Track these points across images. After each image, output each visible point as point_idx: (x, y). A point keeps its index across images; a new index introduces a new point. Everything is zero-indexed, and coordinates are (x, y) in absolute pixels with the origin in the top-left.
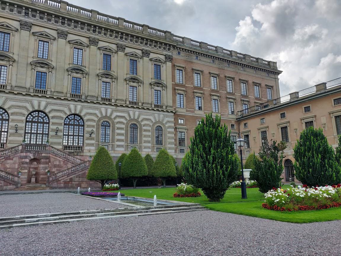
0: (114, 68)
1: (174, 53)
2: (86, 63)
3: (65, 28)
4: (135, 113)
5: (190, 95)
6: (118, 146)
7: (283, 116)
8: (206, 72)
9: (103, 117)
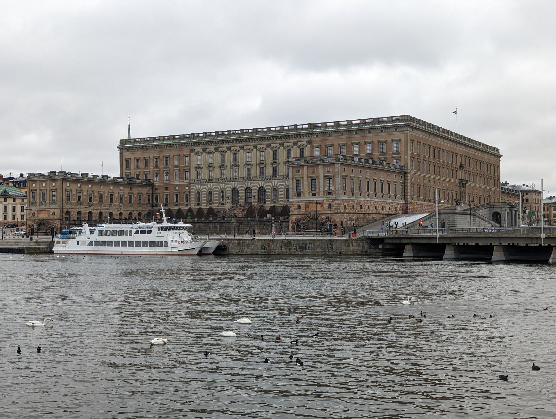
1: (314, 138)
6: (281, 201)
9: (273, 186)
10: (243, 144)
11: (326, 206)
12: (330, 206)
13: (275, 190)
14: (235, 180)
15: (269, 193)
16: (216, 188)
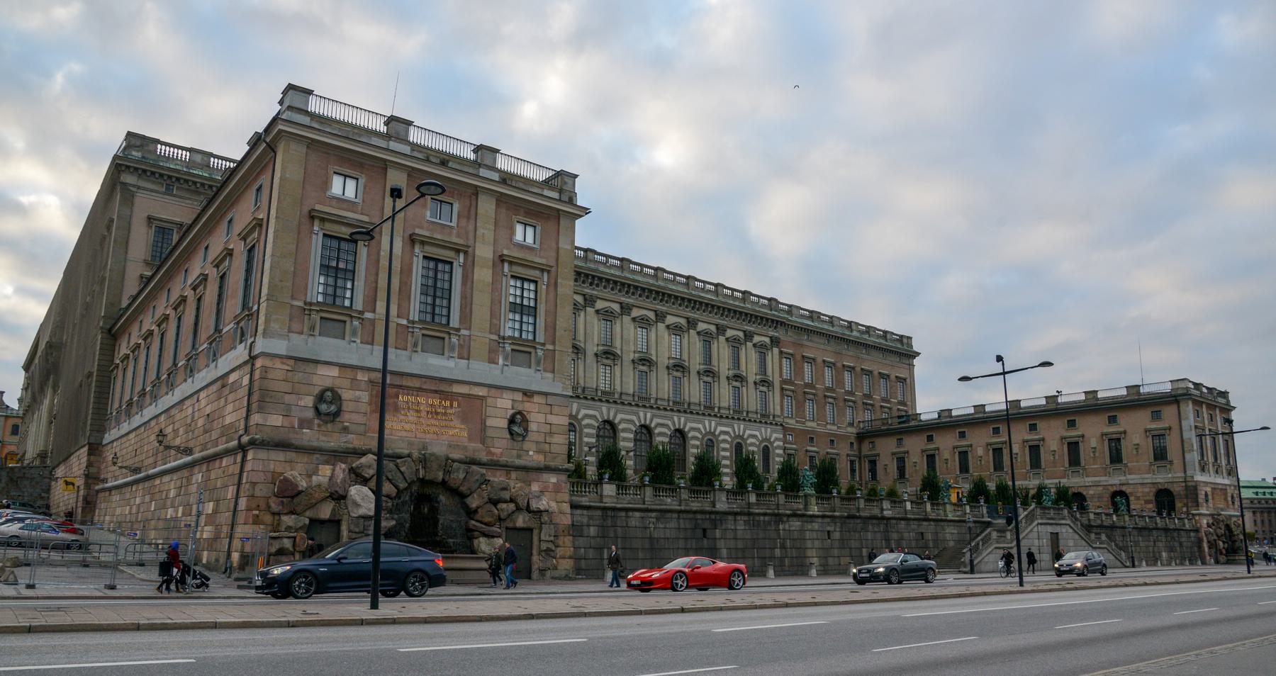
2: (685, 357)
3: (662, 308)
5: (801, 398)
7: (930, 439)
8: (819, 360)
10: (630, 301)
14: (607, 397)
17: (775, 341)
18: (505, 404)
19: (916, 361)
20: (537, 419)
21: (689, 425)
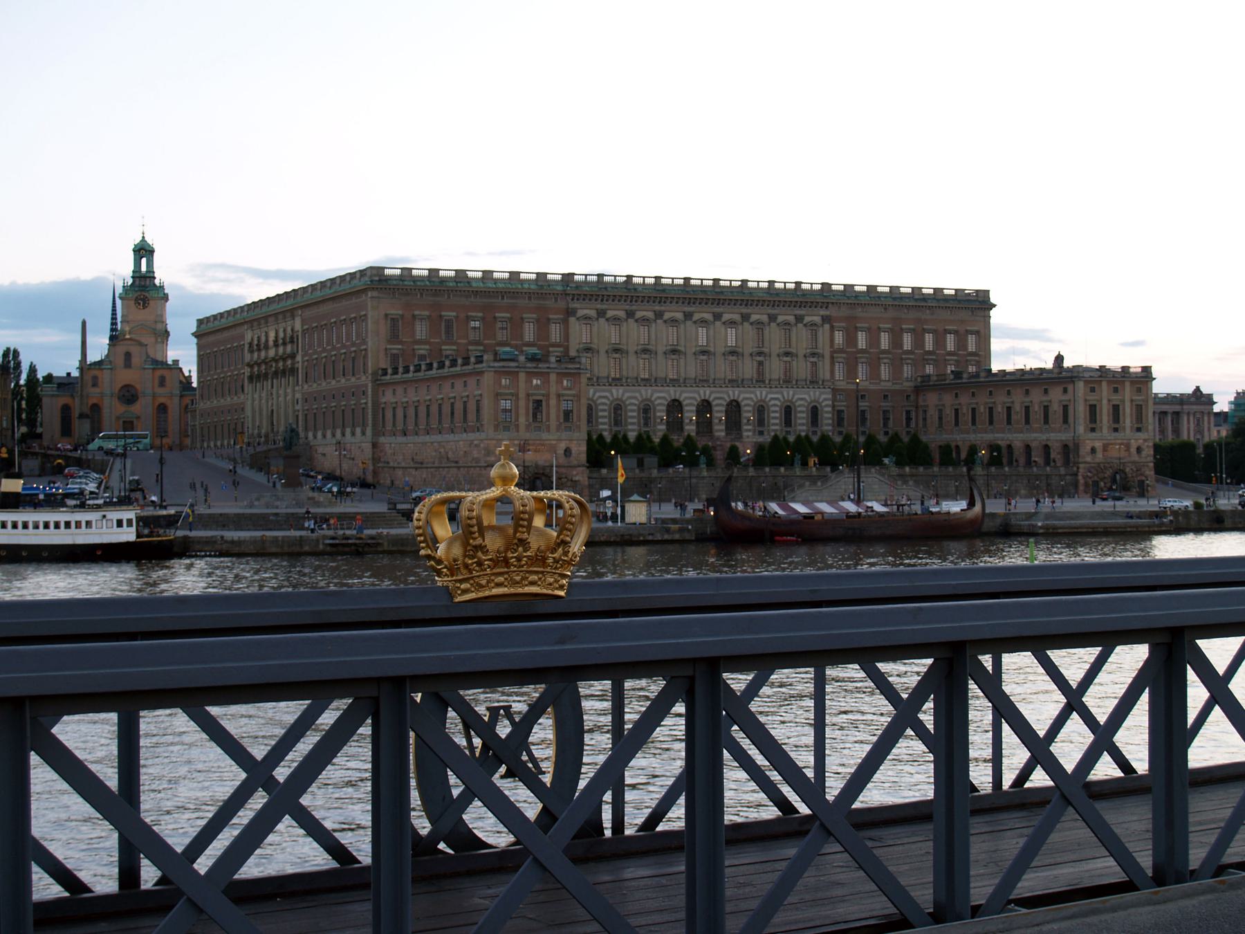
0: (766, 344)
2: (740, 343)
4: (788, 393)
11: (1133, 450)
12: (1139, 450)
13: (761, 410)
15: (748, 414)
16: (633, 397)
17: (826, 319)
18: (563, 445)
19: (992, 313)
20: (574, 450)
21: (742, 396)
